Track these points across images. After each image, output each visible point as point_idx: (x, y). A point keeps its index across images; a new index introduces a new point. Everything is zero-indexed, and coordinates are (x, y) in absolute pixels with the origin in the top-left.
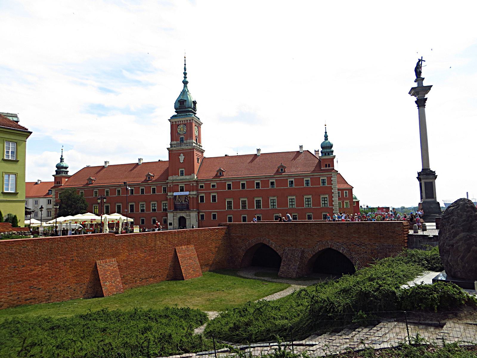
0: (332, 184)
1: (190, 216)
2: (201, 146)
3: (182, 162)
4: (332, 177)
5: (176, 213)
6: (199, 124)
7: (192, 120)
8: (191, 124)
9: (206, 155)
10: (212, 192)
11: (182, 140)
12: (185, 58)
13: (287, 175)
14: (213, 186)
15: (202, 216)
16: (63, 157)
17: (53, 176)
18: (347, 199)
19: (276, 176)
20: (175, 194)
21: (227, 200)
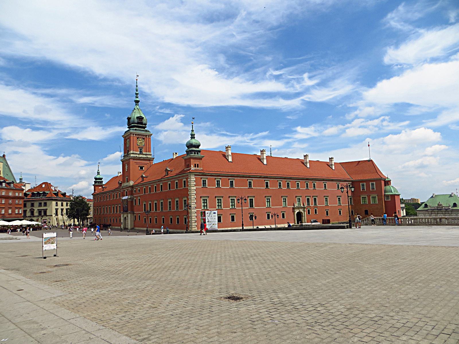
0: (188, 186)
1: (128, 217)
2: (151, 155)
3: (126, 171)
4: (188, 178)
5: (123, 214)
6: (146, 136)
7: (131, 134)
8: (130, 137)
9: (155, 162)
10: (137, 196)
11: (128, 152)
12: (137, 80)
13: (167, 179)
14: (139, 190)
15: (135, 216)
16: (100, 171)
17: (93, 185)
18: (373, 192)
19: (162, 180)
20: (124, 198)
21: (144, 203)
